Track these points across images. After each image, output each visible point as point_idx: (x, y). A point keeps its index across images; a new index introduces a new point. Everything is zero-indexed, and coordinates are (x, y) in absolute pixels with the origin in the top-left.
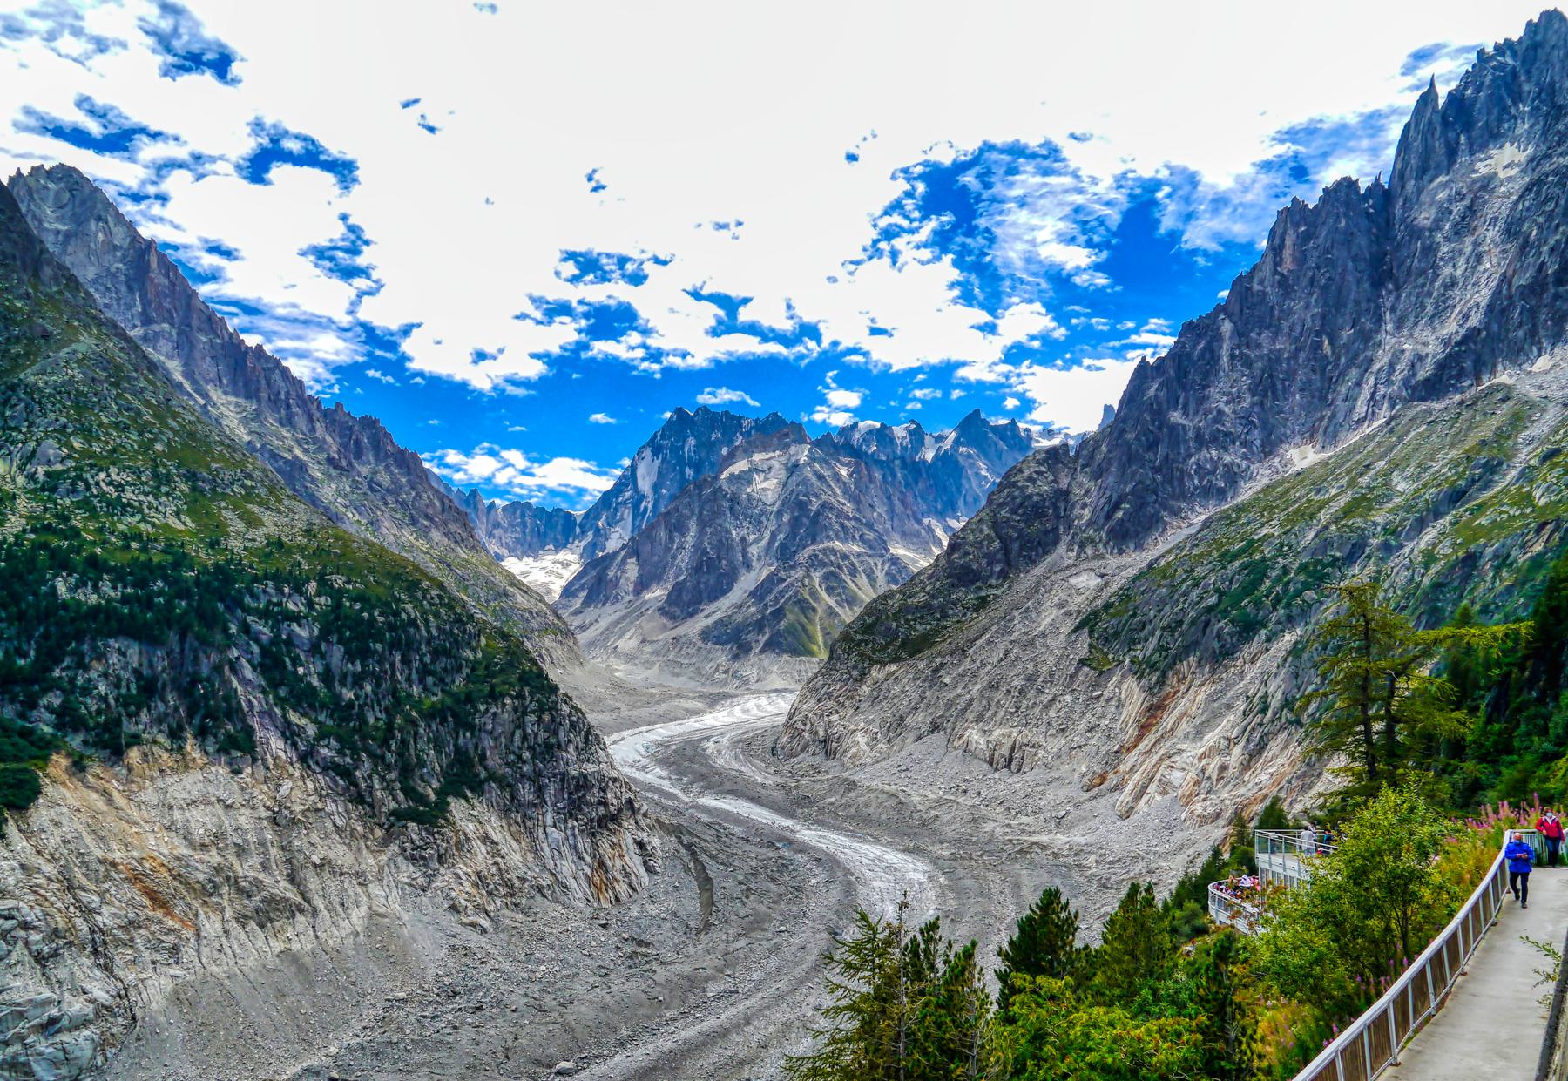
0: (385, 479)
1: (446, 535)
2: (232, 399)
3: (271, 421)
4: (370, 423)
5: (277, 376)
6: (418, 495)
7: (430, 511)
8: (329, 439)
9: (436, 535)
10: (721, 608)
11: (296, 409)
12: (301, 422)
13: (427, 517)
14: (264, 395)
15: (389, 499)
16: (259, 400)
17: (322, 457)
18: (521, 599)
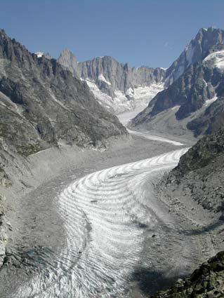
0: (56, 83)
1: (77, 101)
2: (3, 60)
3: (15, 66)
4: (53, 61)
5: (19, 49)
6: (68, 88)
7: (71, 93)
8: (37, 70)
9: (73, 102)
10: (195, 115)
11: (25, 61)
12: (27, 66)
13: (71, 96)
14: (14, 57)
15: (57, 90)
16: (11, 60)
17: (31, 78)
18: (104, 123)
